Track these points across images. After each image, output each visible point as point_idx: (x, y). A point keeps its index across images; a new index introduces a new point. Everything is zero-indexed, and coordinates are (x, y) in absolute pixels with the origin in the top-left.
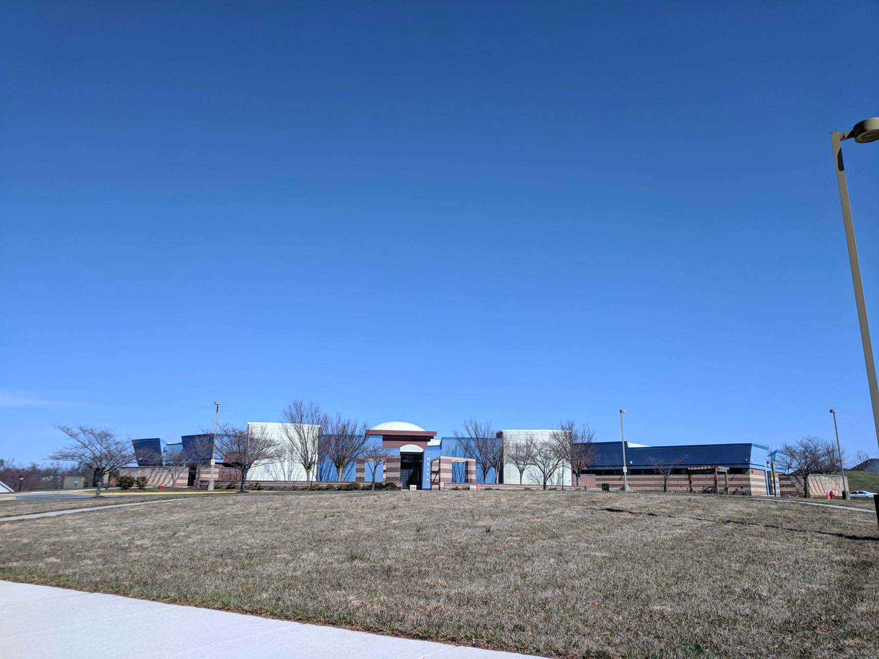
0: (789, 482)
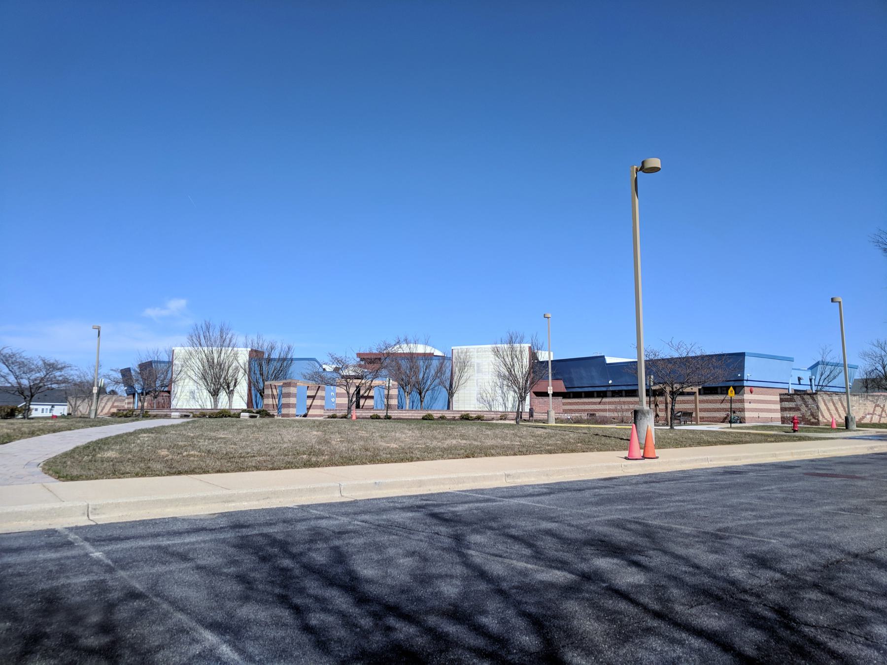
0: (792, 405)
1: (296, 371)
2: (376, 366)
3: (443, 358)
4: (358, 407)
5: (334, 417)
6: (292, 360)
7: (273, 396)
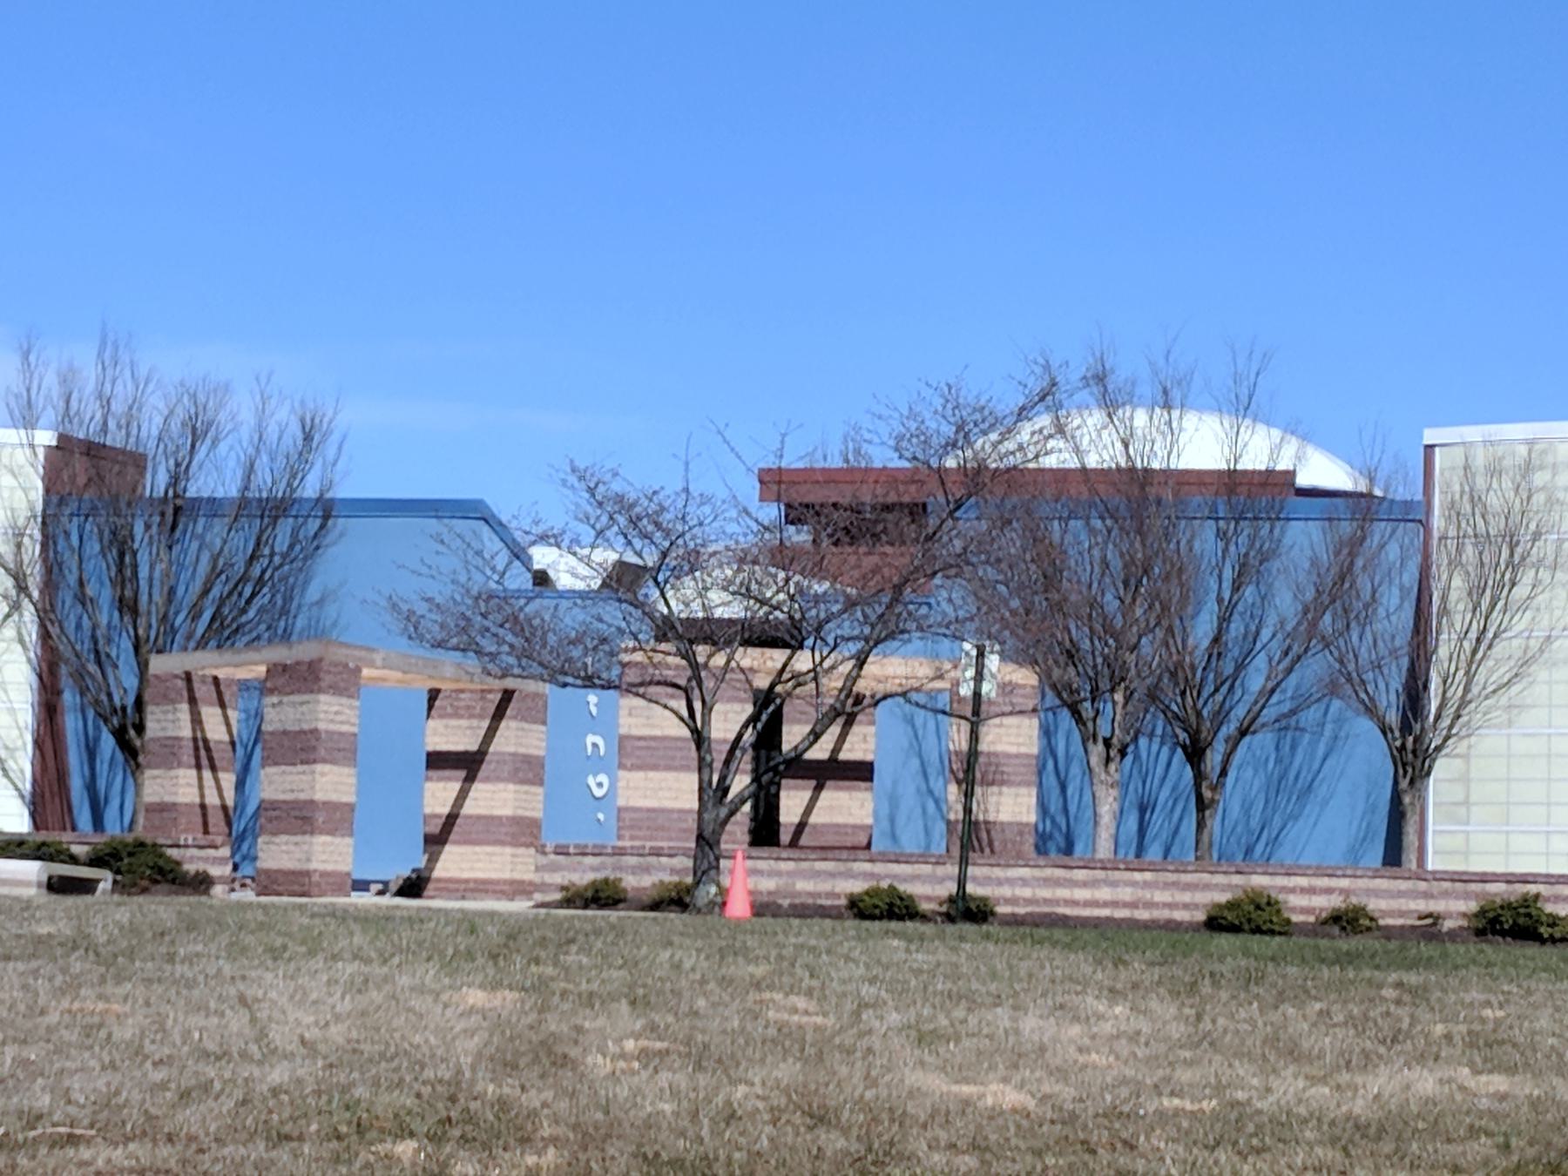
1: (356, 581)
2: (896, 558)
3: (1360, 508)
4: (765, 832)
5: (602, 897)
6: (327, 509)
7: (203, 754)
